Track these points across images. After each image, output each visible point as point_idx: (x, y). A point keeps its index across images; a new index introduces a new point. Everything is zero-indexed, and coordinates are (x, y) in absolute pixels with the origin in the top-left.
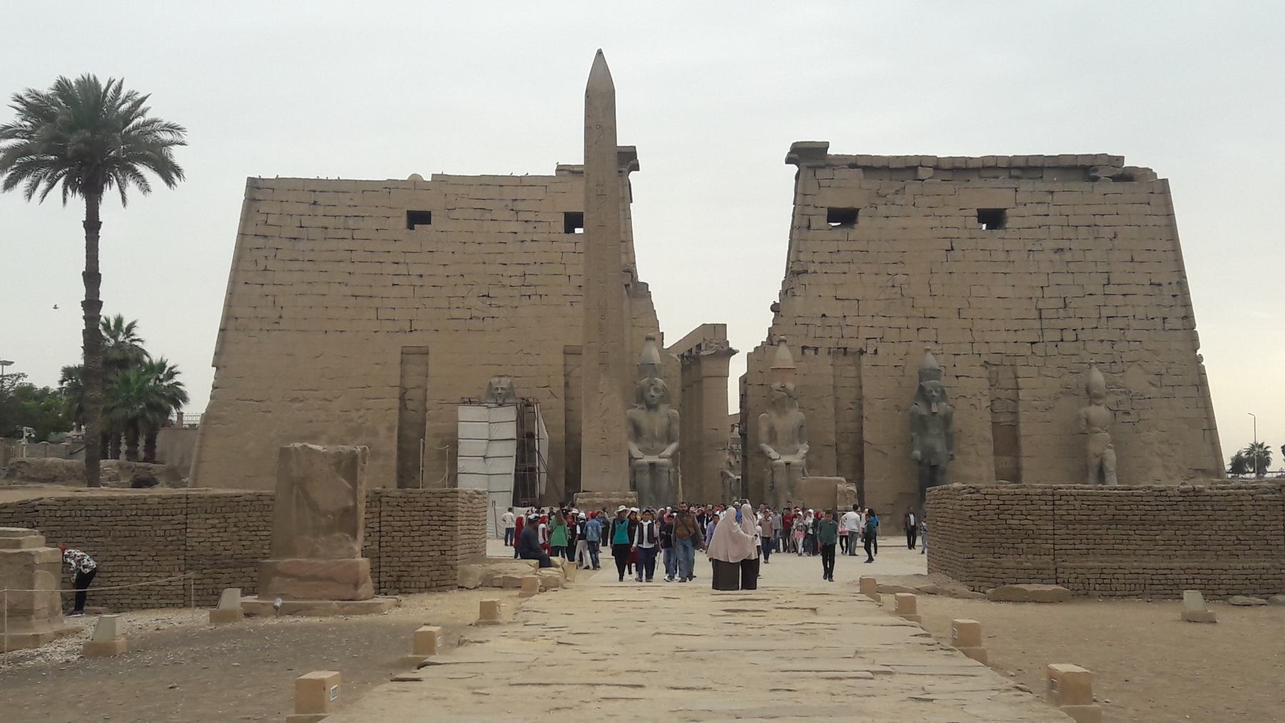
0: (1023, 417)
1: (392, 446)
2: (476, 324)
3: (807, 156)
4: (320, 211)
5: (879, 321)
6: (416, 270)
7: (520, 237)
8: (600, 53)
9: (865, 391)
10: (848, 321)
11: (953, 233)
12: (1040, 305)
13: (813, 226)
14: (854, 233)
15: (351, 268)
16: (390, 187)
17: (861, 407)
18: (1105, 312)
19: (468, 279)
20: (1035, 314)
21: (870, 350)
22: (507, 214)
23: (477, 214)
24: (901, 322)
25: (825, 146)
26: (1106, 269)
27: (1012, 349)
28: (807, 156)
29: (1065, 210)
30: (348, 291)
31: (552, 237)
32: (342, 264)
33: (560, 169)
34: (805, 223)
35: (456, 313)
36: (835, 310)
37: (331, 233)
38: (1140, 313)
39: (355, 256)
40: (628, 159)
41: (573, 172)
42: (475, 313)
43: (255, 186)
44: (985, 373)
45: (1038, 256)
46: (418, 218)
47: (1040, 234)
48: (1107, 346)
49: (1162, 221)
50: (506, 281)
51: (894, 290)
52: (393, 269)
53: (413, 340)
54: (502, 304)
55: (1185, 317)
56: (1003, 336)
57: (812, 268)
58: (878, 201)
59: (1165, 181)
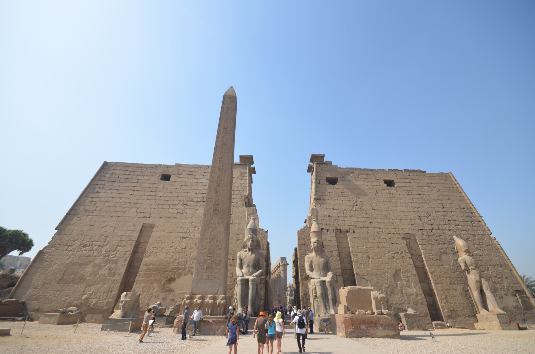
2: (179, 215)
4: (127, 173)
5: (353, 219)
7: (203, 184)
11: (377, 187)
12: (419, 214)
13: (321, 182)
14: (336, 186)
15: (132, 192)
18: (447, 218)
19: (179, 198)
20: (418, 218)
21: (352, 231)
23: (189, 176)
24: (362, 219)
26: (440, 202)
27: (413, 232)
29: (418, 181)
30: (127, 201)
35: (170, 211)
36: (334, 213)
37: (129, 180)
39: (135, 189)
42: (179, 211)
44: (404, 242)
46: (166, 178)
51: (357, 207)
53: (149, 221)
56: (408, 227)
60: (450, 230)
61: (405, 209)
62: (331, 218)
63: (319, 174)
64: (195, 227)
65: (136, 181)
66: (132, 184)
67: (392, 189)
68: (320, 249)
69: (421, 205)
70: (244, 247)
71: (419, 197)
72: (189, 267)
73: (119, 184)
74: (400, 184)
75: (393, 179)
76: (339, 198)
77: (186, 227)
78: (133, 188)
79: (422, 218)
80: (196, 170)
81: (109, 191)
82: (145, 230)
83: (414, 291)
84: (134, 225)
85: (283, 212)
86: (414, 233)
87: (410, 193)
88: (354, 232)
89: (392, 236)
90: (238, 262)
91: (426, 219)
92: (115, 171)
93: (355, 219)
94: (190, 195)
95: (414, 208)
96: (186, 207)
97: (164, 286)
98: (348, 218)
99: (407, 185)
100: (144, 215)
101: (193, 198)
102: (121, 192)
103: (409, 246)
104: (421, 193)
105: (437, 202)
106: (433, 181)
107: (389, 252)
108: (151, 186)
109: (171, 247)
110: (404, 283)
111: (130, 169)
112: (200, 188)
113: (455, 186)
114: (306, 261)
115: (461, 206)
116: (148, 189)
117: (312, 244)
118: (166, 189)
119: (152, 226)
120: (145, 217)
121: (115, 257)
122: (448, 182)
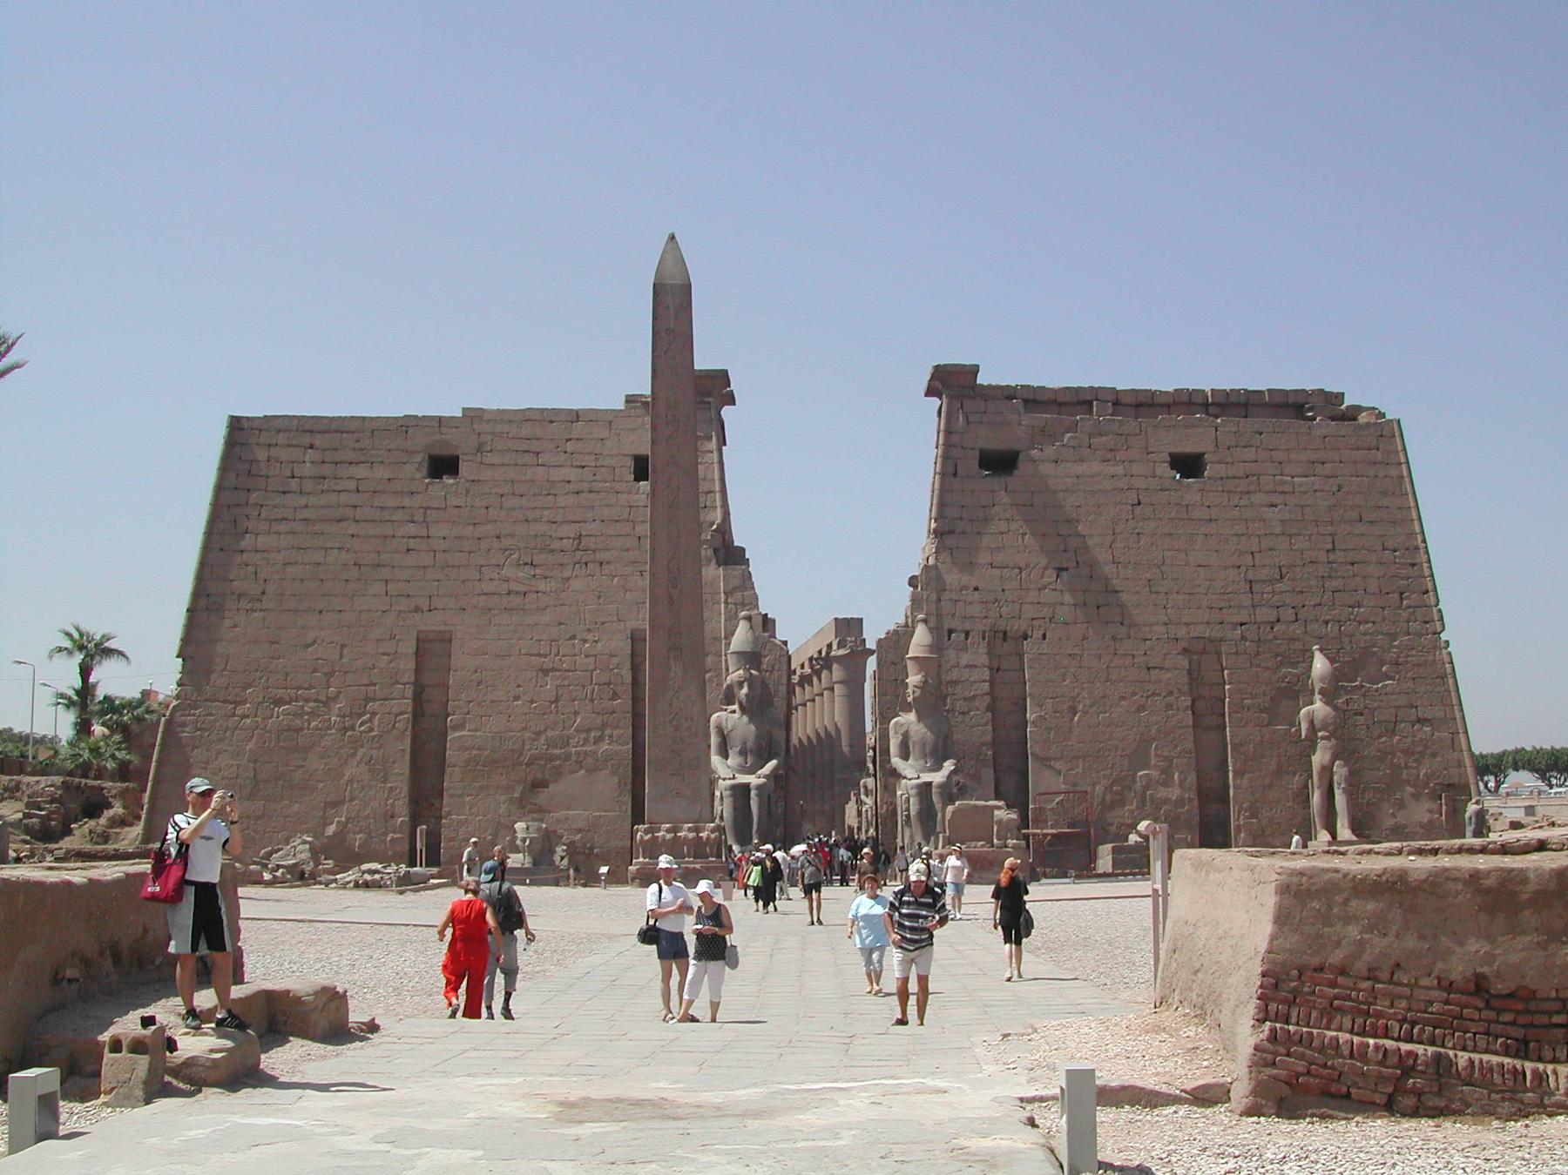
2: (518, 600)
3: (952, 384)
7: (572, 487)
8: (673, 237)
11: (1139, 483)
12: (1250, 576)
15: (353, 529)
16: (406, 425)
21: (1038, 634)
25: (974, 370)
28: (952, 384)
31: (617, 486)
32: (342, 525)
33: (630, 400)
34: (952, 471)
35: (488, 587)
38: (1373, 586)
39: (359, 513)
40: (717, 388)
43: (236, 424)
50: (555, 545)
53: (431, 623)
54: (548, 573)
60: (1327, 622)
64: (573, 637)
65: (351, 485)
66: (343, 498)
68: (933, 704)
70: (729, 698)
72: (578, 753)
73: (303, 501)
74: (1221, 470)
75: (1201, 450)
77: (545, 637)
78: (350, 512)
79: (1256, 588)
80: (538, 432)
81: (283, 527)
82: (431, 652)
83: (1174, 793)
84: (393, 637)
85: (833, 537)
86: (1219, 635)
87: (1243, 502)
88: (1044, 637)
89: (1152, 648)
90: (714, 740)
91: (1269, 589)
92: (274, 452)
94: (535, 528)
95: (1241, 553)
96: (529, 571)
97: (521, 798)
98: (1032, 596)
102: (319, 527)
103: (1194, 675)
105: (1322, 529)
107: (1134, 693)
108: (407, 502)
109: (517, 698)
110: (1154, 773)
111: (318, 440)
112: (562, 501)
113: (1393, 472)
114: (891, 732)
116: (398, 516)
117: (910, 690)
118: (454, 511)
119: (446, 639)
120: (417, 609)
121: (372, 729)
122: (1379, 456)
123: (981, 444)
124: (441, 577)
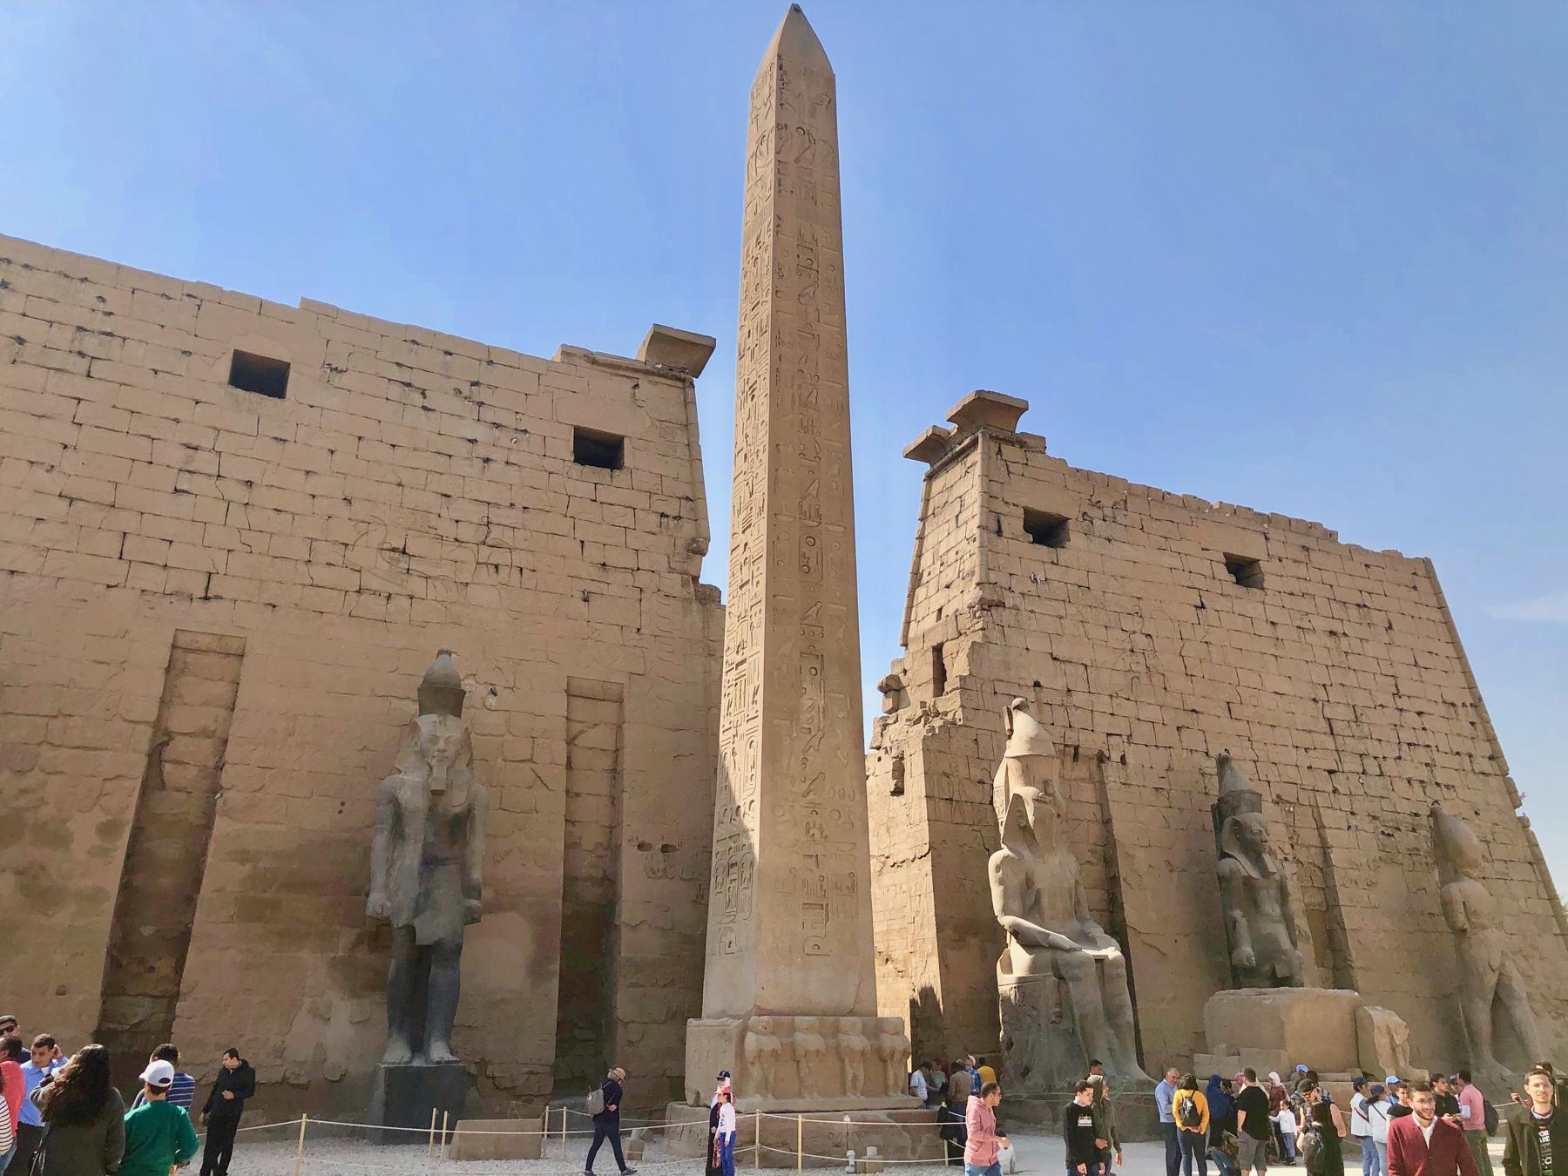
0: (1343, 896)
1: (110, 877)
2: (376, 606)
6: (237, 470)
7: (481, 451)
9: (1119, 829)
10: (1078, 699)
11: (1199, 582)
13: (1004, 528)
14: (1064, 555)
17: (1109, 861)
18: (1406, 736)
20: (1324, 726)
21: (1116, 756)
22: (456, 404)
23: (395, 391)
25: (1017, 409)
27: (1308, 779)
29: (1329, 577)
30: (54, 483)
33: (567, 353)
35: (321, 574)
41: (594, 362)
45: (1310, 638)
46: (260, 377)
47: (1305, 604)
48: (1416, 785)
49: (1437, 616)
50: (448, 530)
52: (178, 456)
55: (1491, 758)
56: (1293, 756)
57: (1009, 602)
58: (1094, 513)
59: (1427, 563)
61: (1284, 687)
62: (1046, 696)
63: (995, 488)
67: (1248, 602)
69: (1337, 676)
71: (1330, 642)
76: (1071, 609)
87: (1306, 625)
88: (1123, 759)
93: (1128, 709)
99: (1296, 586)
100: (174, 581)
101: (434, 522)
104: (1337, 626)
106: (1377, 588)
115: (1450, 700)
123: (1025, 502)
124: (233, 543)
